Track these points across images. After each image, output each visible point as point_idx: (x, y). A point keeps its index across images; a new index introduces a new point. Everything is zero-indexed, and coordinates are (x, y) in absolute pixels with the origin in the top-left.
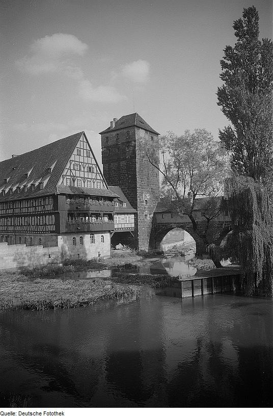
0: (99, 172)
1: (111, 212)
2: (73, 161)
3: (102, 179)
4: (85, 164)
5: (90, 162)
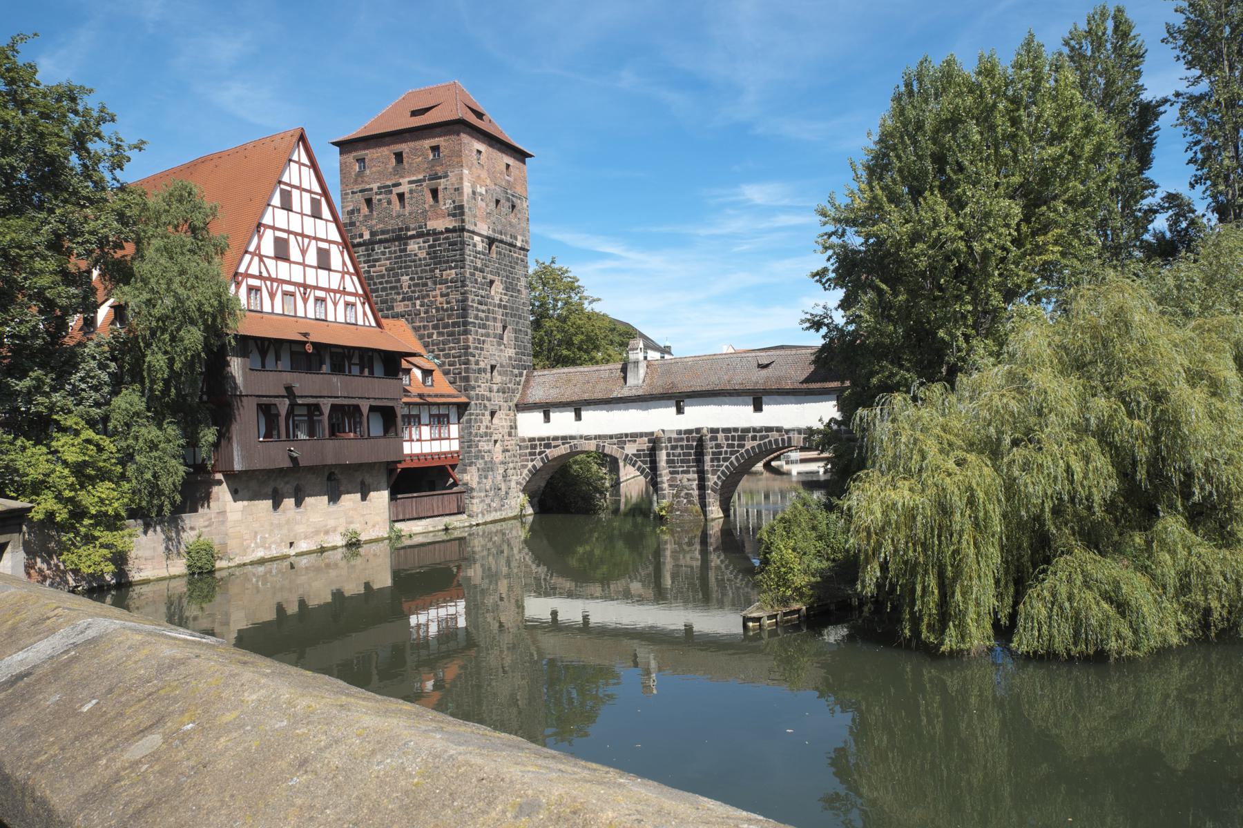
0: (352, 270)
1: (390, 404)
3: (360, 291)
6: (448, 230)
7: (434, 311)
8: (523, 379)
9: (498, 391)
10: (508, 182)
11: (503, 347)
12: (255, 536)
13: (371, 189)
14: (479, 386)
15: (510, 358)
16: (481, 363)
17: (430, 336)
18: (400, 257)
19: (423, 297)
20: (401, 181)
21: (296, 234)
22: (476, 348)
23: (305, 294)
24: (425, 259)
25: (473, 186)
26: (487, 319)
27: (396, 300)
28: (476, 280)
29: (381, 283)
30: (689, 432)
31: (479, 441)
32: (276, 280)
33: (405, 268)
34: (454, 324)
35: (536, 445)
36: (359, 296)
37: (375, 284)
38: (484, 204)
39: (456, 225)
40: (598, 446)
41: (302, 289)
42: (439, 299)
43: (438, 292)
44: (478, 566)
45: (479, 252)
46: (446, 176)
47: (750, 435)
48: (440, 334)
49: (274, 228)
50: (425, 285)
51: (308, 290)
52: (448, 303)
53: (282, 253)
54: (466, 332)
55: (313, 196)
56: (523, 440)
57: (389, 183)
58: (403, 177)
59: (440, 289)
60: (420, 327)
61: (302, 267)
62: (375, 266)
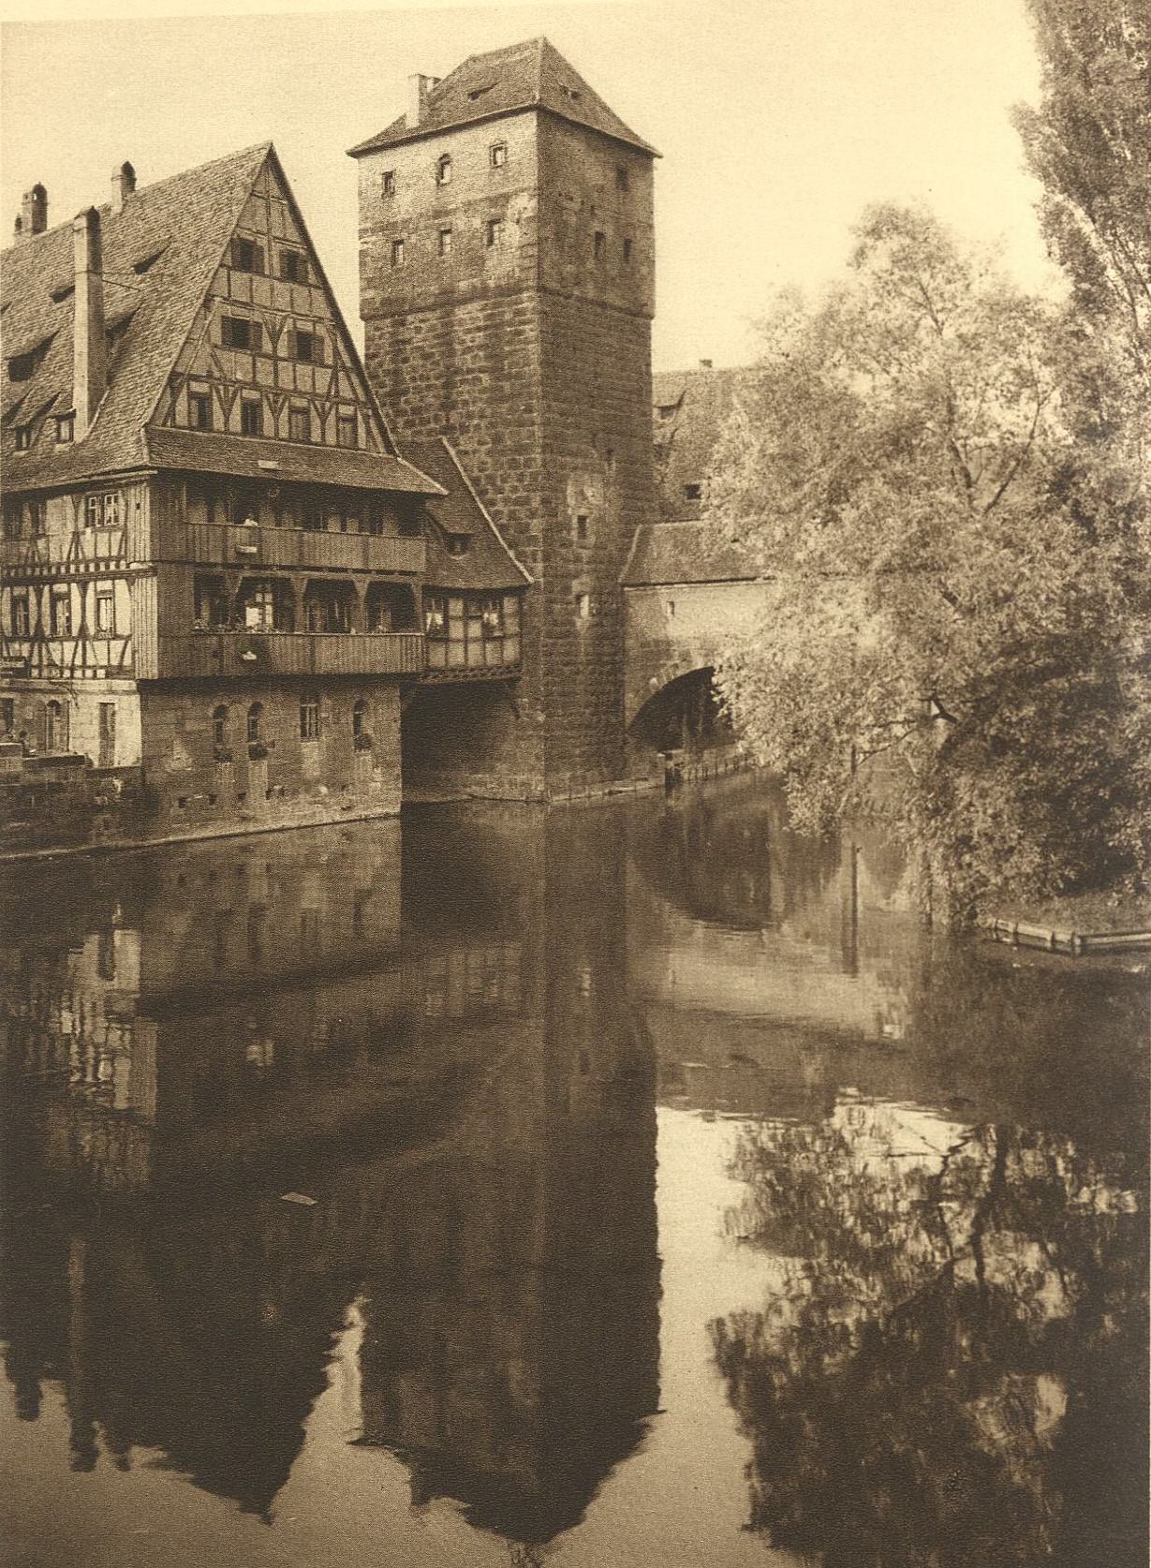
3: (362, 398)
23: (276, 402)
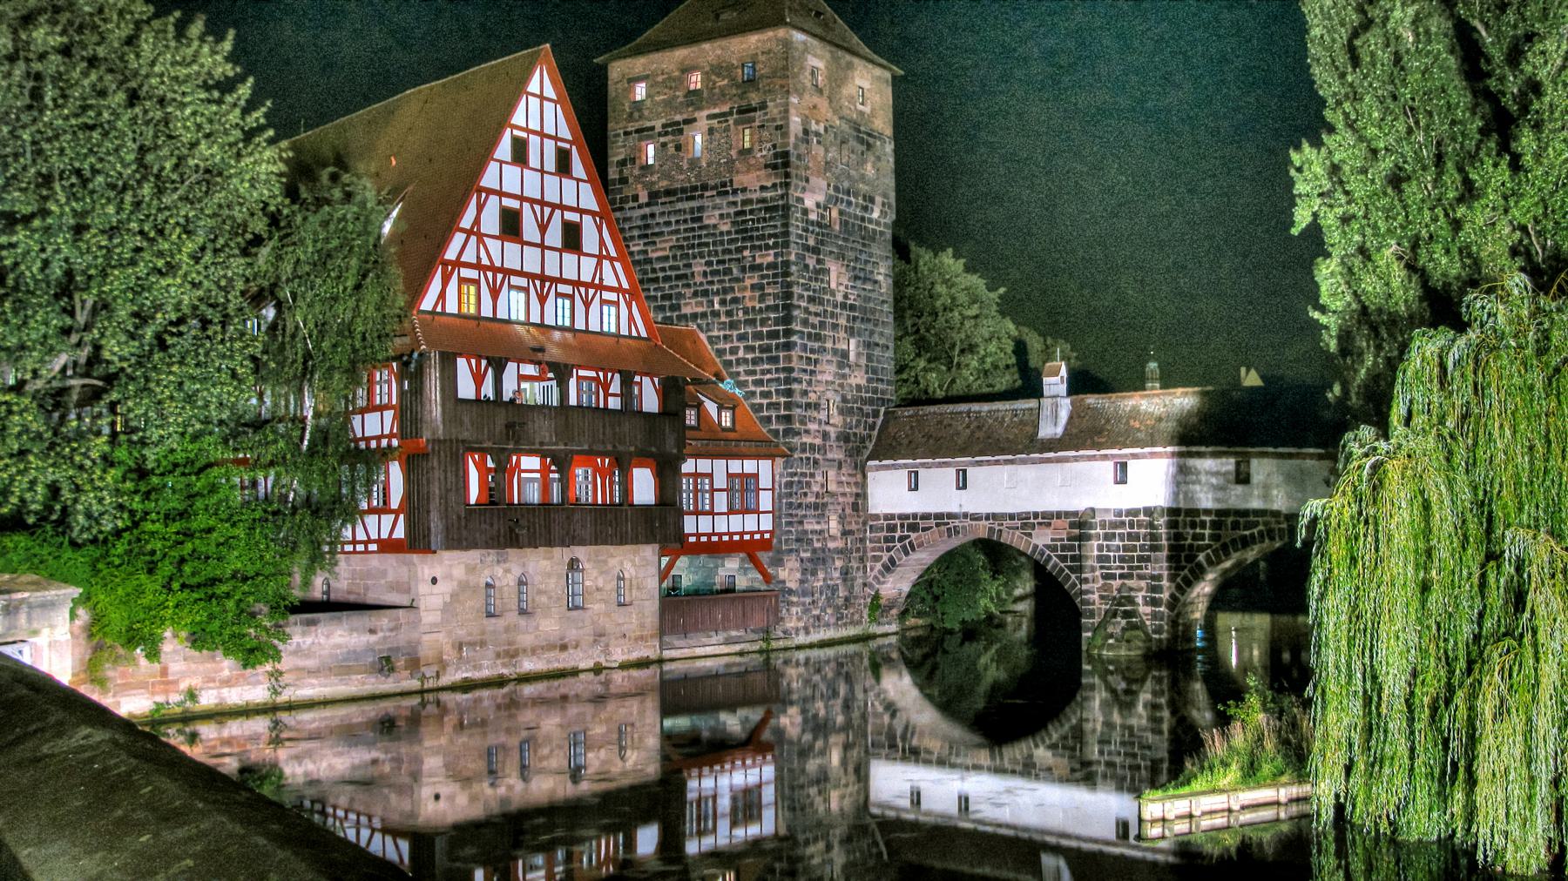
0: (613, 254)
2: (490, 192)
3: (625, 285)
4: (547, 210)
5: (569, 200)
6: (763, 188)
7: (741, 313)
8: (879, 422)
9: (838, 439)
10: (862, 113)
11: (847, 371)
12: (460, 649)
13: (653, 128)
14: (807, 432)
15: (859, 387)
16: (812, 395)
17: (734, 351)
18: (693, 229)
19: (725, 291)
20: (696, 115)
21: (532, 201)
22: (805, 371)
23: (542, 287)
24: (729, 233)
25: (805, 121)
26: (822, 325)
27: (680, 296)
28: (806, 266)
29: (663, 269)
30: (1133, 512)
31: (805, 516)
32: (502, 270)
33: (699, 245)
34: (773, 335)
35: (895, 525)
36: (624, 292)
37: (654, 271)
38: (821, 151)
39: (778, 181)
40: (991, 530)
41: (538, 283)
42: (748, 294)
43: (748, 283)
44: (793, 711)
45: (812, 223)
46: (763, 106)
47: (1230, 519)
48: (746, 348)
49: (501, 194)
50: (728, 271)
51: (547, 284)
52: (762, 299)
53: (511, 226)
54: (788, 346)
55: (559, 144)
56: (876, 517)
57: (678, 118)
58: (700, 109)
59: (749, 278)
60: (718, 337)
61: (539, 250)
62: (654, 243)
